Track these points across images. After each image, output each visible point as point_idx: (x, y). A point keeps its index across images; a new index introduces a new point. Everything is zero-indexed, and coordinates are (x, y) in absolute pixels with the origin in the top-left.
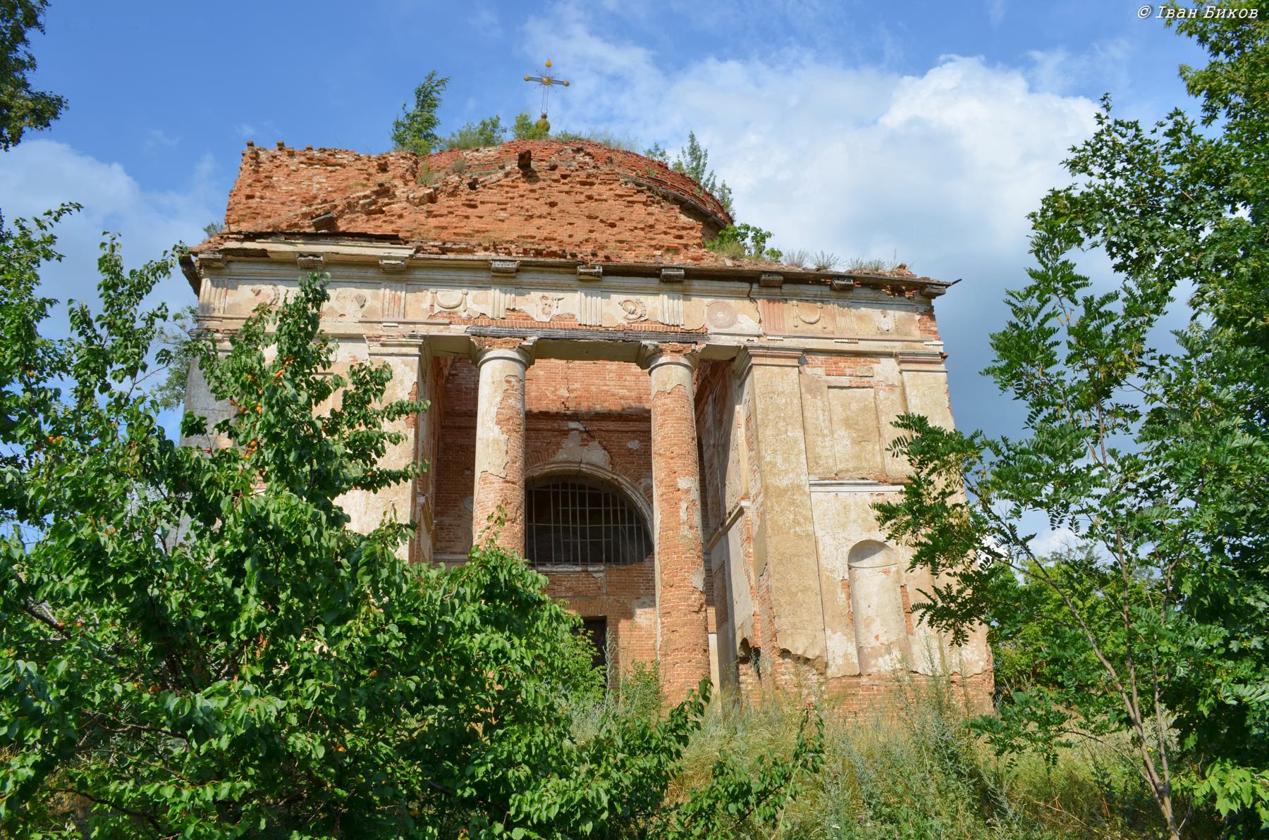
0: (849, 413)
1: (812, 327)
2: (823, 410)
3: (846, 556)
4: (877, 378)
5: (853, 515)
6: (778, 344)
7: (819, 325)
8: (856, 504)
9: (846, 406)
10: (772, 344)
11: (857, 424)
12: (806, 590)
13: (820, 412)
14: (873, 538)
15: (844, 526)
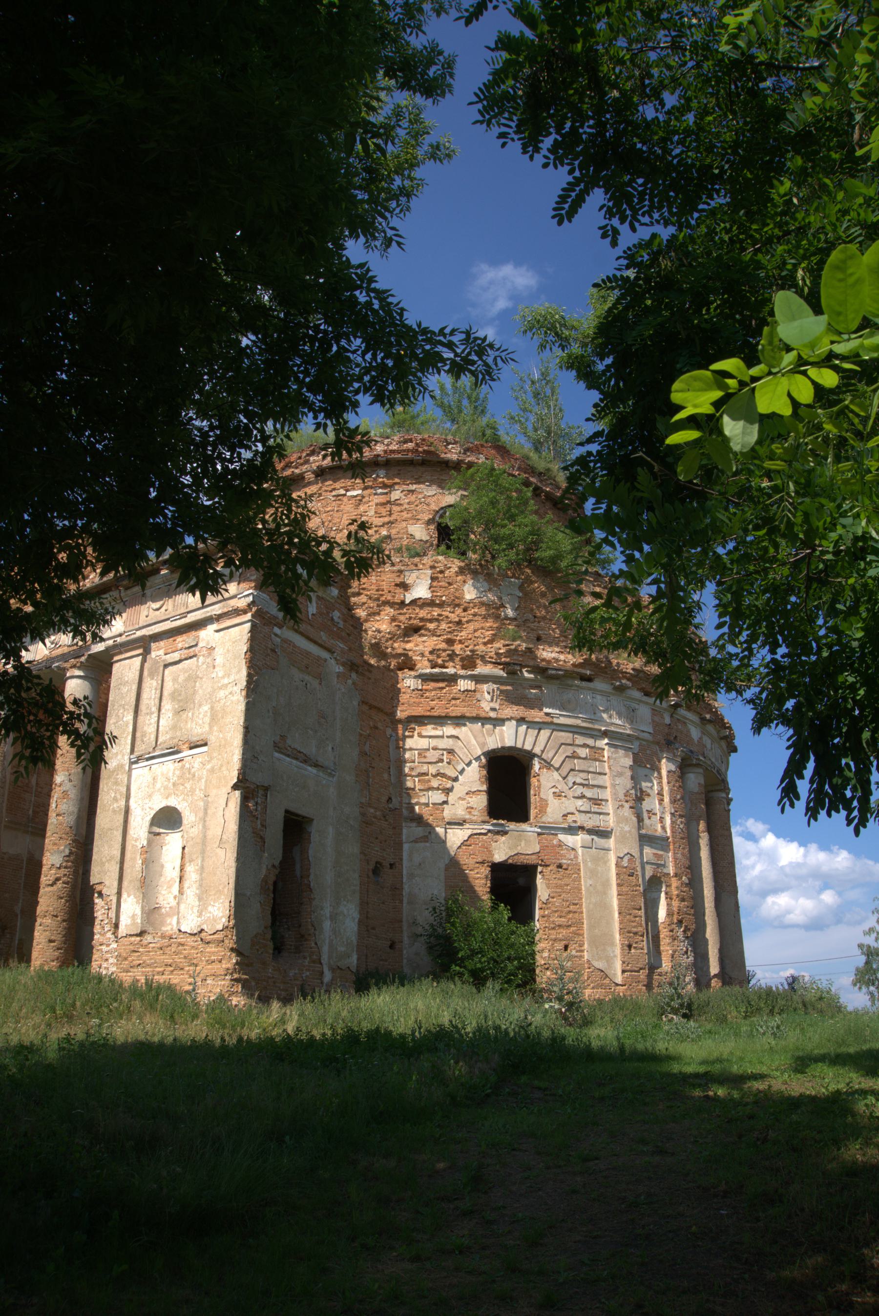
0: (176, 686)
1: (158, 613)
2: (156, 689)
3: (147, 823)
4: (201, 645)
5: (158, 785)
6: (133, 637)
7: (163, 610)
8: (162, 774)
9: (175, 680)
10: (129, 638)
11: (180, 695)
12: (112, 858)
13: (153, 691)
14: (169, 804)
15: (150, 796)
